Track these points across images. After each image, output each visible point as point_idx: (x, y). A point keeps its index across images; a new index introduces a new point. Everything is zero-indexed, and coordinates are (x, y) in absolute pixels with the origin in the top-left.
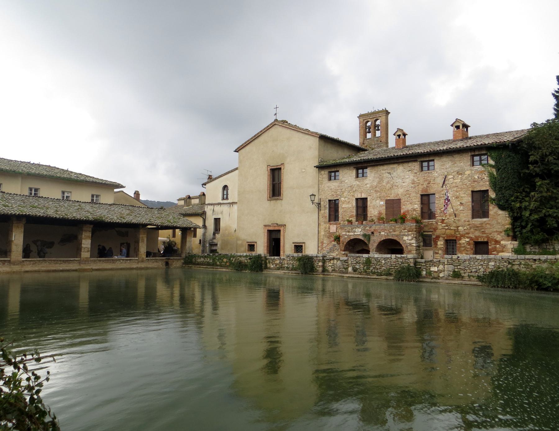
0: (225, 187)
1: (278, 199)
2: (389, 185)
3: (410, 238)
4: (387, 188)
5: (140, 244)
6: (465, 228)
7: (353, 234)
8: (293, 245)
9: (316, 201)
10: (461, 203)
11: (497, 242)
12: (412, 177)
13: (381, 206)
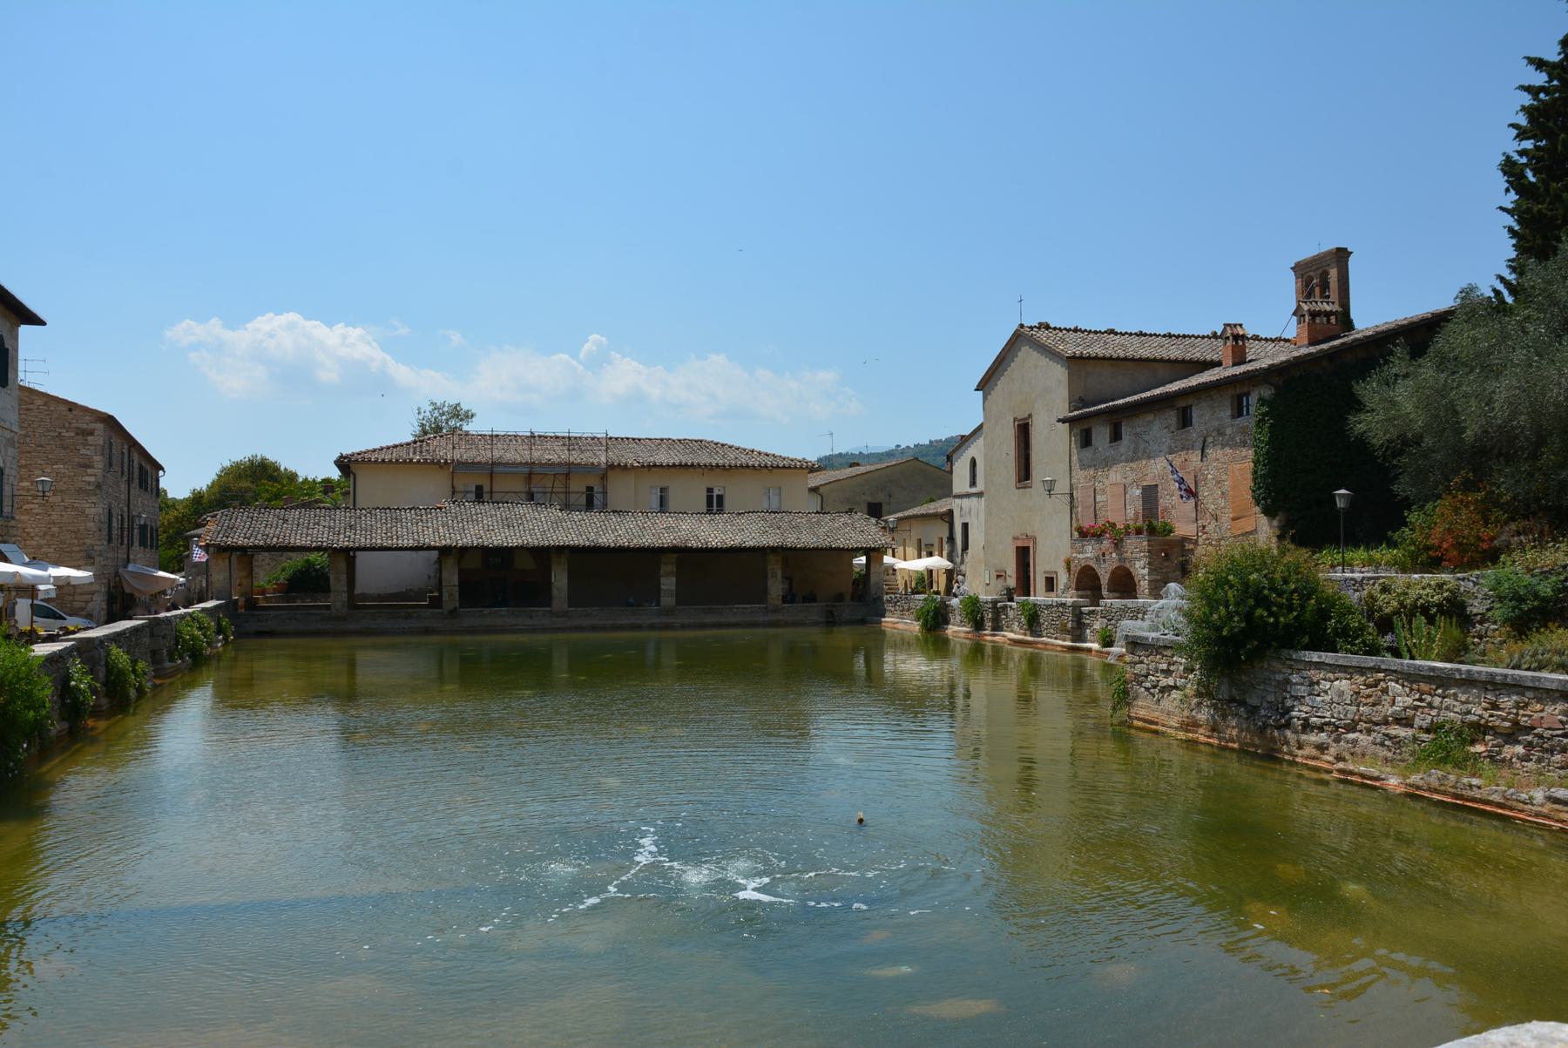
0: (973, 463)
5: (770, 583)
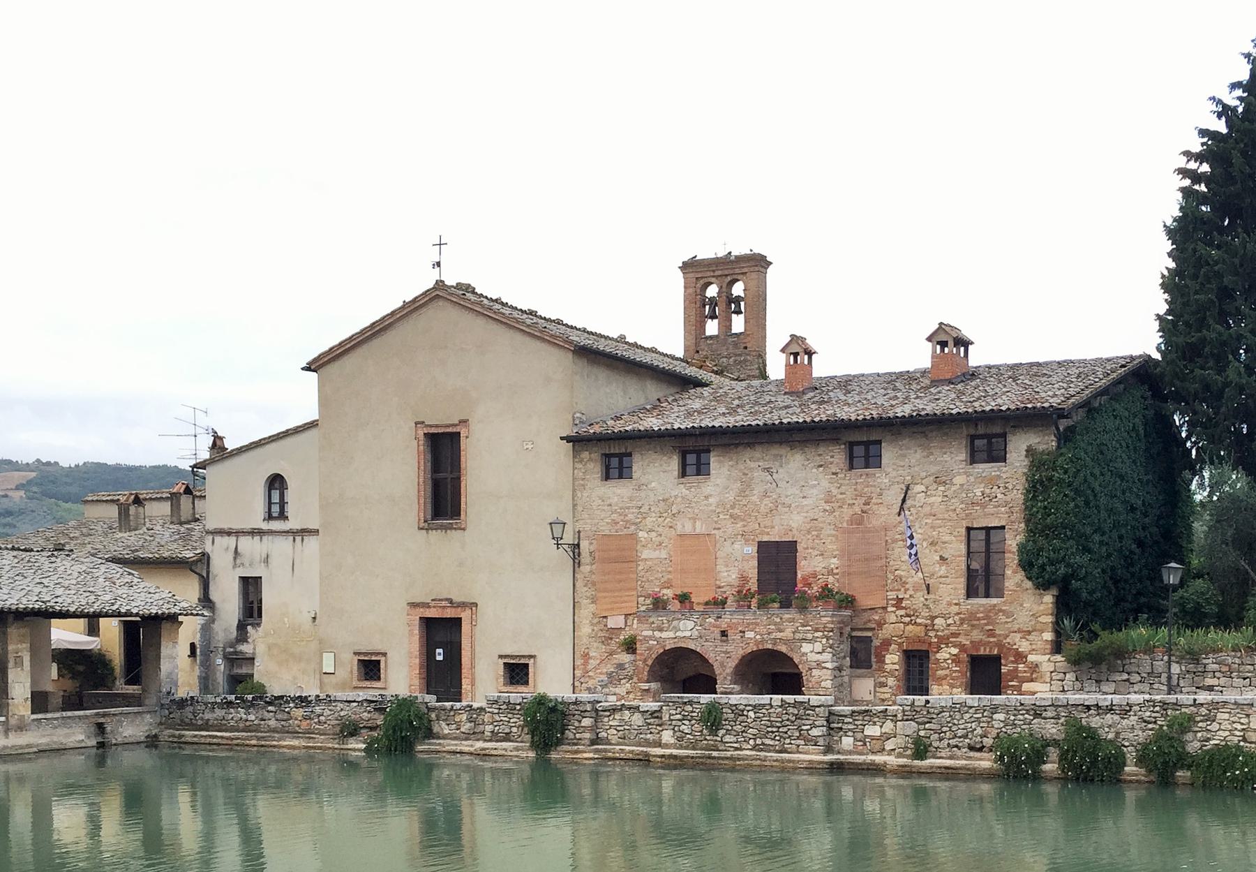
0: (276, 482)
1: (450, 527)
2: (766, 501)
3: (818, 647)
4: (763, 509)
6: (950, 621)
7: (671, 634)
8: (501, 662)
9: (569, 538)
10: (942, 558)
11: (1020, 657)
12: (825, 484)
13: (745, 559)
